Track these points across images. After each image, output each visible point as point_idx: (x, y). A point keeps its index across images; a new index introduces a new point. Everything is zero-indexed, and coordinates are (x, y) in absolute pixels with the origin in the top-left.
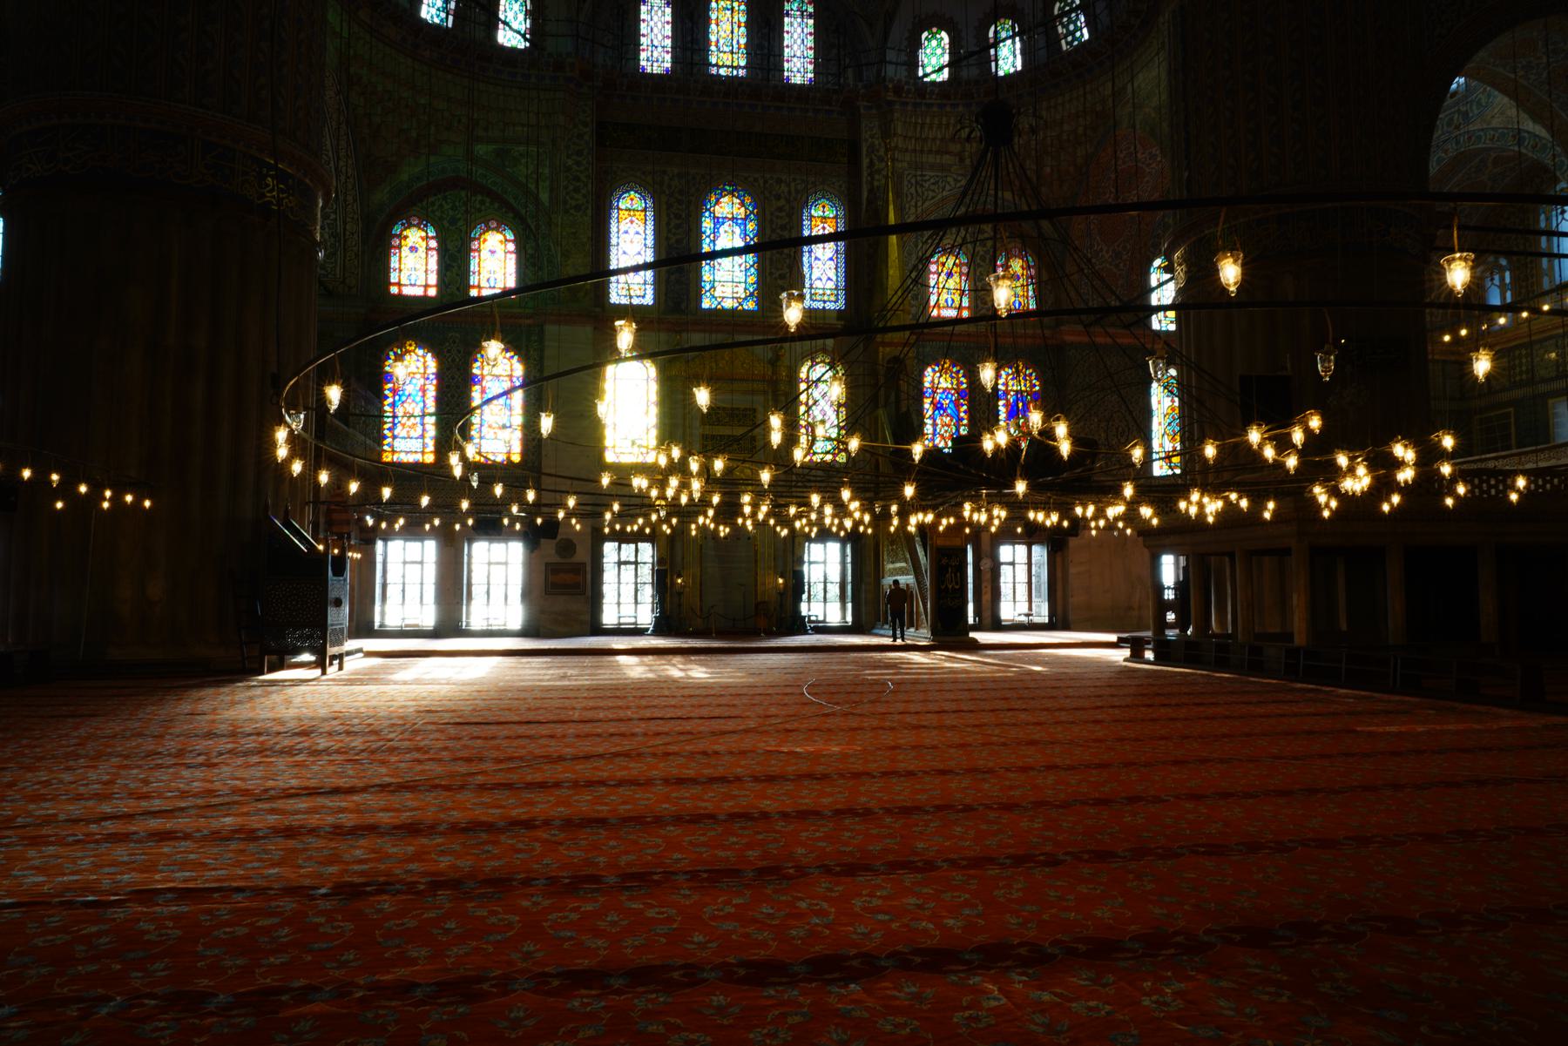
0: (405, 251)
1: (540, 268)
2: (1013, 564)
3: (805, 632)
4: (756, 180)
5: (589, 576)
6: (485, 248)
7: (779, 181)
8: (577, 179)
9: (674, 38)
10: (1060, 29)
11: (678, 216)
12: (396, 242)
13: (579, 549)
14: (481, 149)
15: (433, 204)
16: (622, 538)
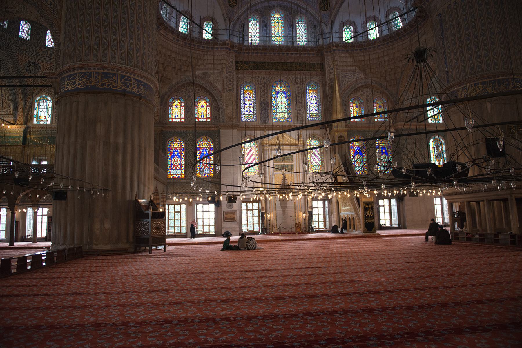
0: (174, 107)
1: (218, 111)
2: (384, 206)
3: (313, 232)
4: (289, 78)
5: (238, 215)
6: (200, 105)
7: (297, 78)
8: (230, 81)
9: (260, 33)
10: (392, 23)
11: (264, 91)
12: (170, 104)
14: (198, 73)
15: (182, 91)
16: (247, 201)
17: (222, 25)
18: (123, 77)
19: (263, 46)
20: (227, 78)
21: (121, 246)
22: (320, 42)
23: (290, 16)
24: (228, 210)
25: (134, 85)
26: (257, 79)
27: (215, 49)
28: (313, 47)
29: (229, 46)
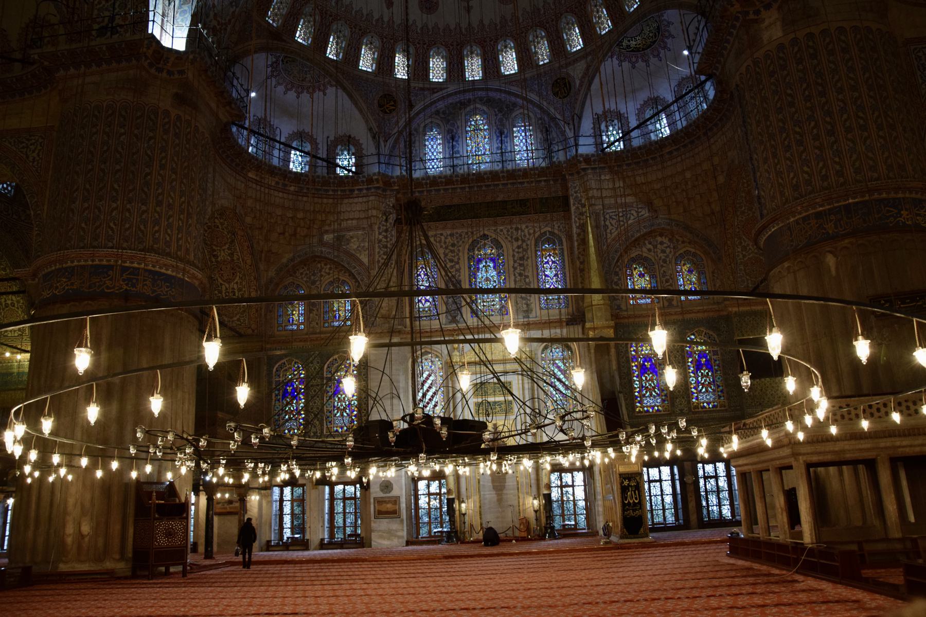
4: (502, 230)
7: (517, 229)
11: (451, 261)
13: (395, 487)
14: (328, 238)
15: (302, 274)
17: (369, 146)
18: (124, 269)
19: (445, 177)
20: (380, 241)
21: (109, 565)
22: (560, 157)
23: (500, 116)
24: (382, 495)
25: (145, 280)
26: (438, 239)
27: (356, 192)
28: (542, 168)
29: (381, 184)
